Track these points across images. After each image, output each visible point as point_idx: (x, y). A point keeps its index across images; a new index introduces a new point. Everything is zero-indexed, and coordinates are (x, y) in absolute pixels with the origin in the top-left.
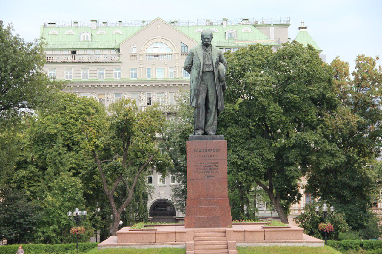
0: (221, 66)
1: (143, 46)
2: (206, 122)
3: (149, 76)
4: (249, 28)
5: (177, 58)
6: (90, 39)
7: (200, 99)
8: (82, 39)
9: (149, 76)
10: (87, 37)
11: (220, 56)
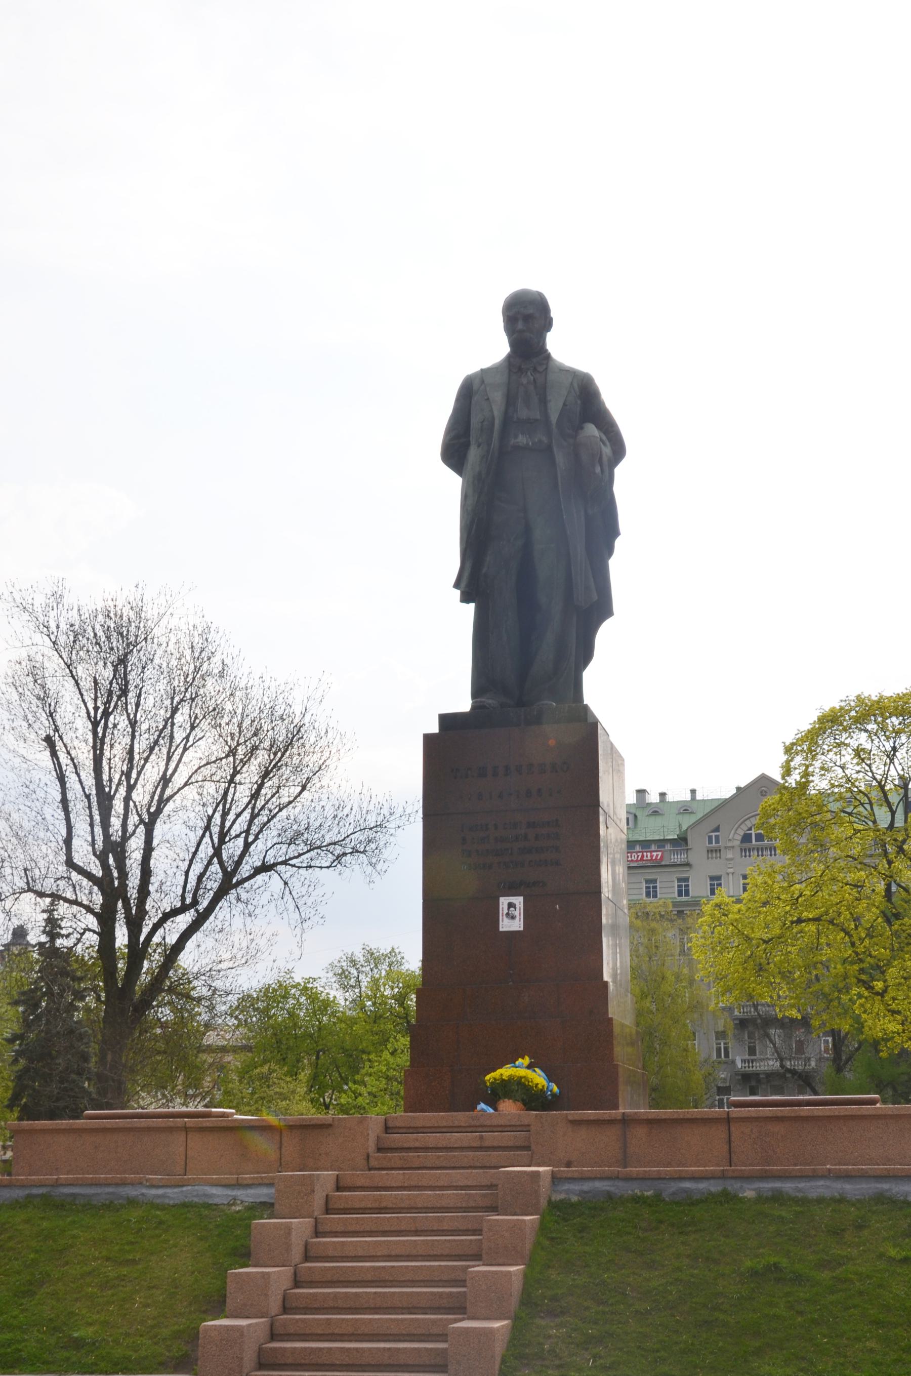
1: (733, 832)
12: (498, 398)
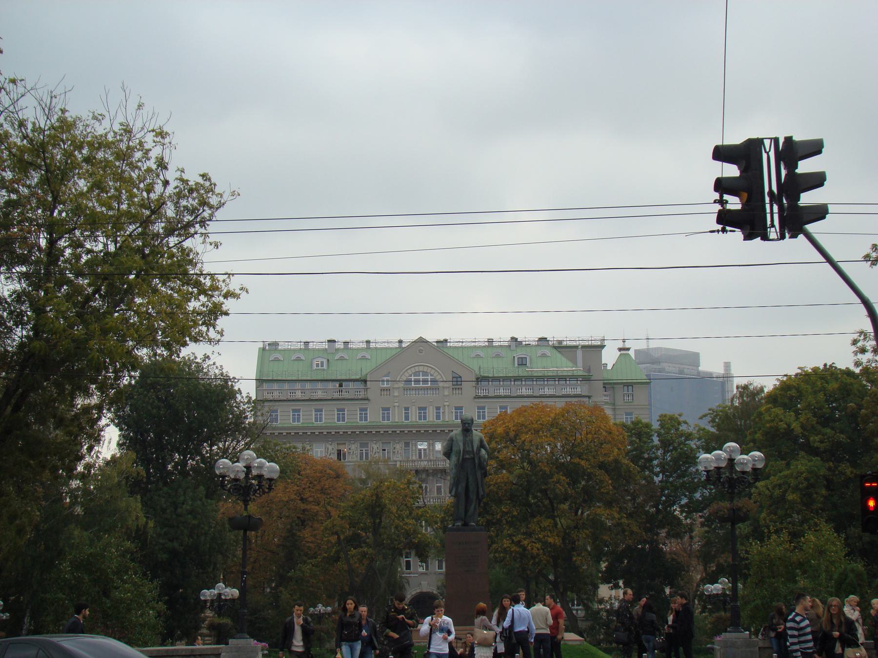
0: (483, 451)
2: (466, 511)
3: (407, 418)
4: (548, 351)
5: (446, 393)
6: (325, 367)
7: (460, 488)
8: (315, 367)
9: (407, 418)
10: (322, 363)
11: (481, 441)
12: (461, 444)
